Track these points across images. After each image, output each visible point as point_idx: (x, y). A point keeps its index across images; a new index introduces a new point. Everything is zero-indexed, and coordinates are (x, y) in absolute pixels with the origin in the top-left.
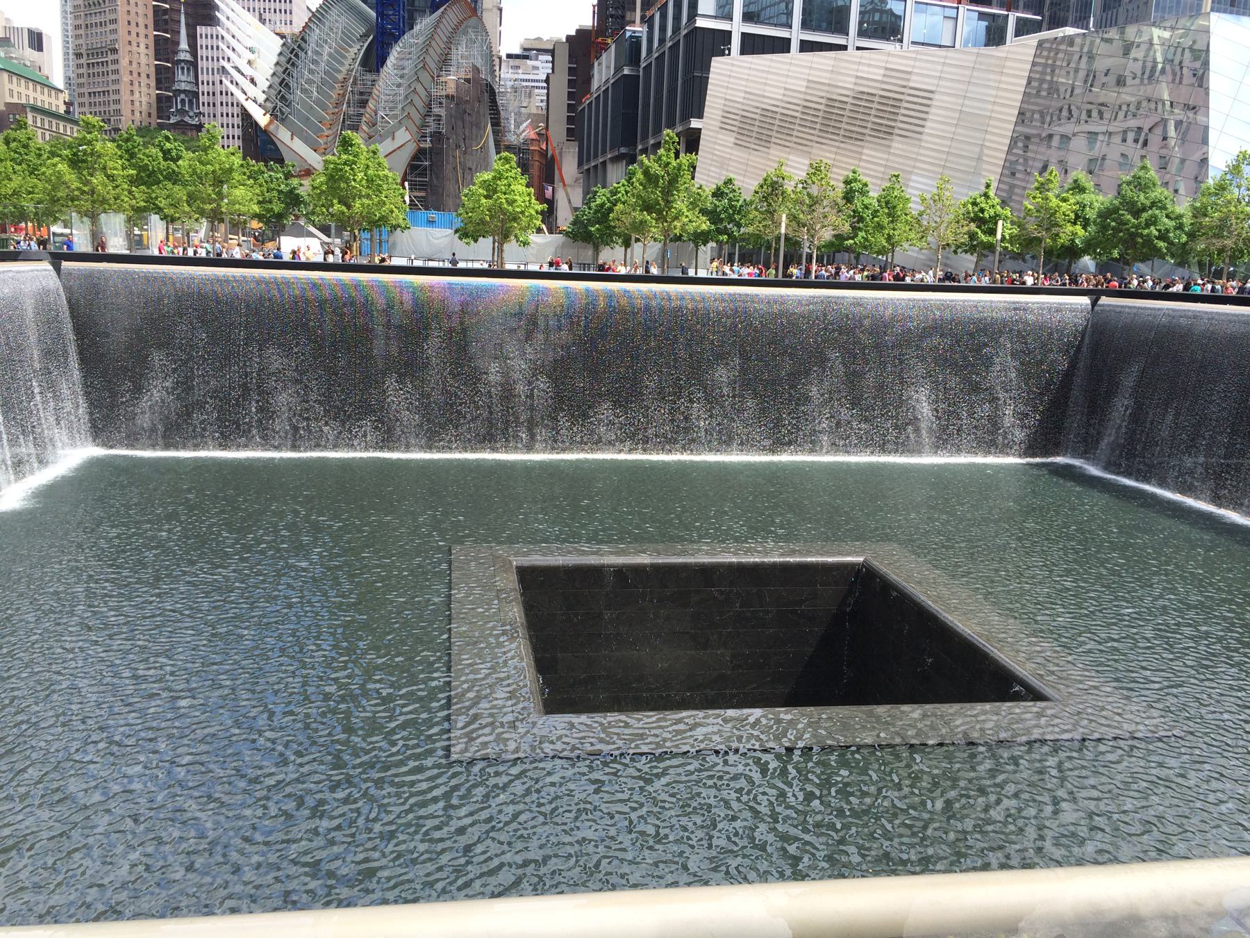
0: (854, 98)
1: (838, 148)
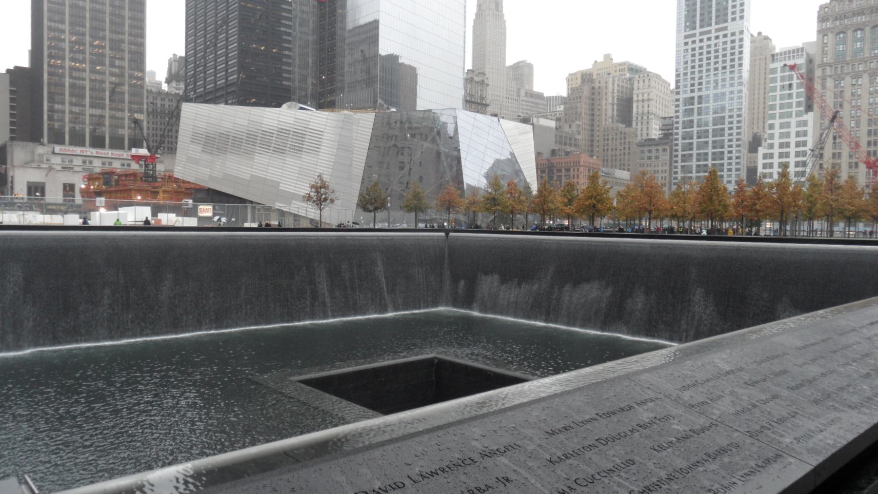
0: (278, 131)
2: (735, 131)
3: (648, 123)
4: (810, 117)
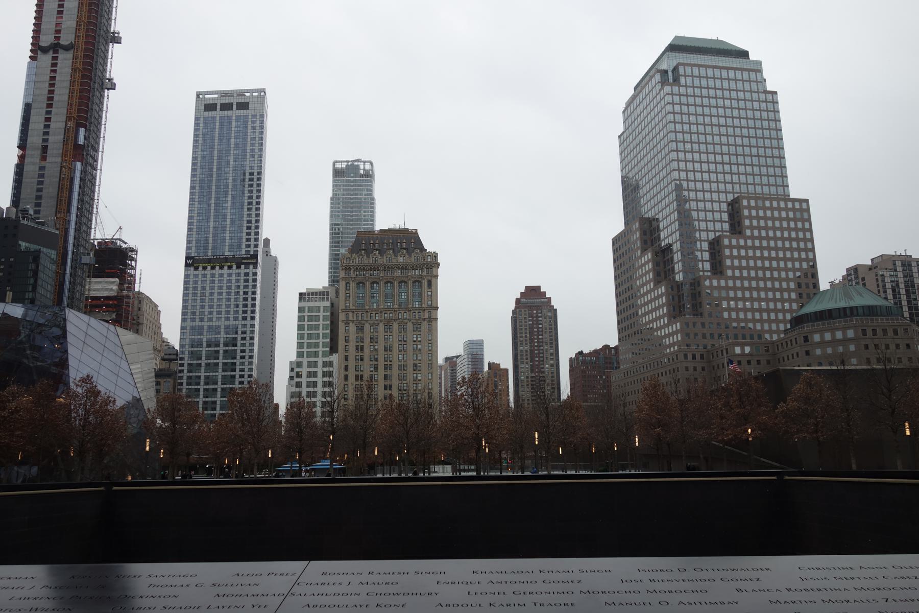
4: (335, 358)
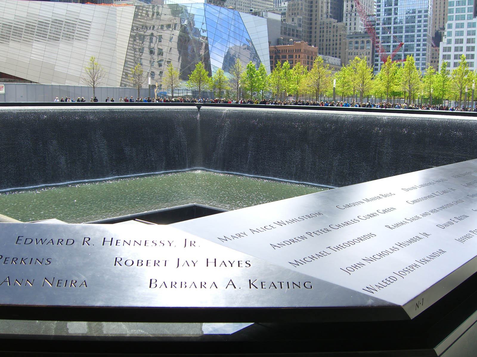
0: (52, 22)
1: (47, 43)
2: (422, 28)
3: (355, 19)
